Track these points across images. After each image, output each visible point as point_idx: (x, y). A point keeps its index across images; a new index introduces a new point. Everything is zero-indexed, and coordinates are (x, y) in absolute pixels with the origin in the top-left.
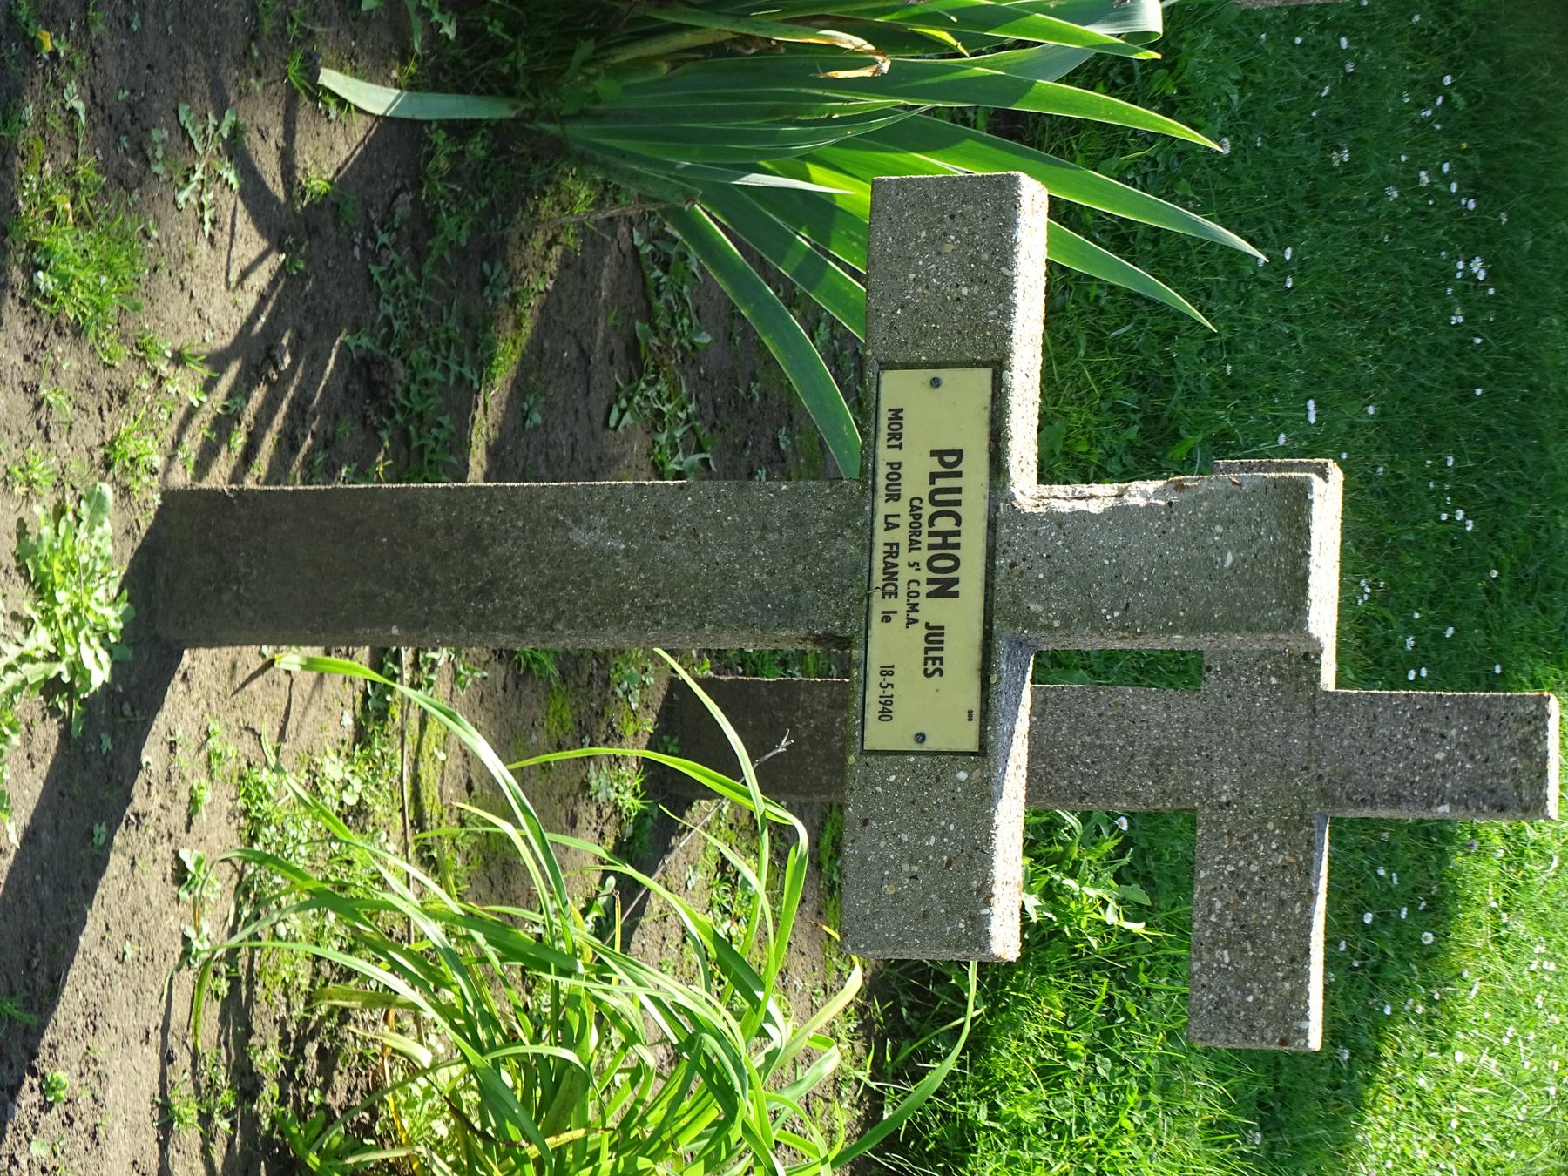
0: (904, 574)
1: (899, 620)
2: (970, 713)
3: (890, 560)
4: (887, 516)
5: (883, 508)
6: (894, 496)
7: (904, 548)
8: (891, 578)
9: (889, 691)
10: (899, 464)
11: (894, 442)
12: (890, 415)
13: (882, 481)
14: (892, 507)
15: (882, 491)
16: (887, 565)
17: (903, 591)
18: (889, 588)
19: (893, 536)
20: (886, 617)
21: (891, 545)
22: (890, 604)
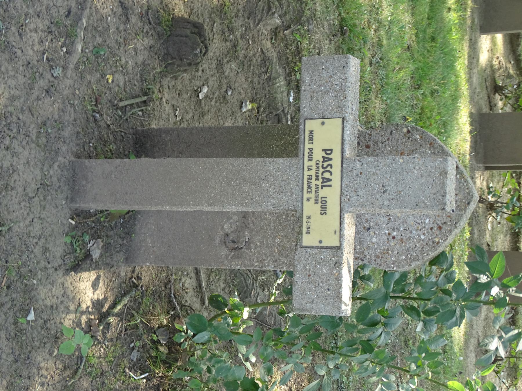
2: (335, 231)
3: (309, 181)
5: (307, 163)
6: (310, 159)
7: (314, 177)
8: (309, 187)
11: (310, 142)
13: (306, 155)
14: (310, 163)
15: (306, 158)
16: (309, 182)
17: (313, 192)
18: (309, 190)
19: (310, 173)
20: (308, 200)
22: (309, 195)
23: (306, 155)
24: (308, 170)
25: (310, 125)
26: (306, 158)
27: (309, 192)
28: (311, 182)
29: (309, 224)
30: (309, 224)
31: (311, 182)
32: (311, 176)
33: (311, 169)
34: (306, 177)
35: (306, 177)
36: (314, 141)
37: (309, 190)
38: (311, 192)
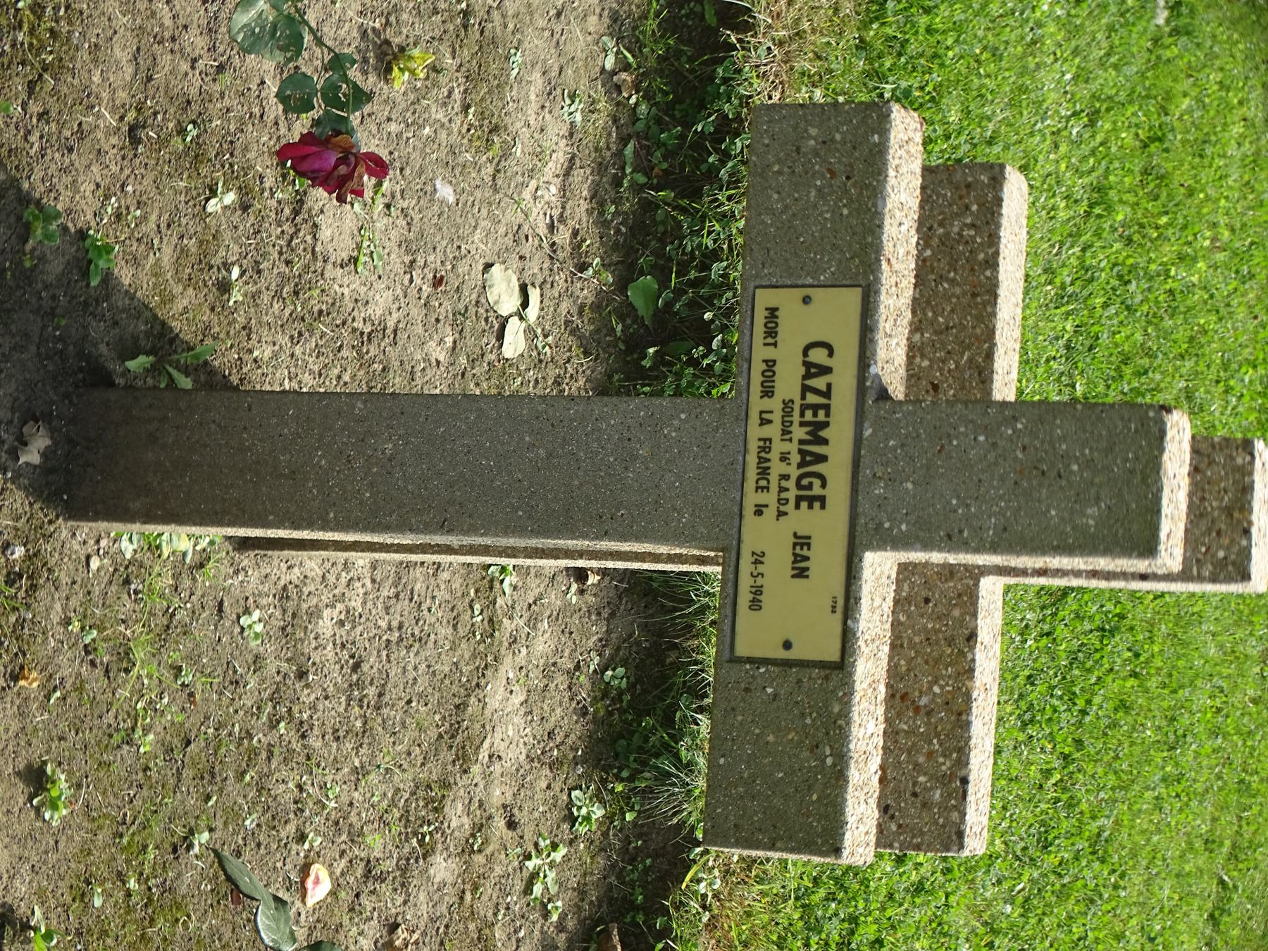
0: (777, 468)
1: (770, 513)
3: (763, 455)
4: (761, 412)
5: (757, 403)
6: (768, 393)
8: (764, 472)
9: (759, 583)
10: (774, 361)
11: (770, 340)
12: (766, 313)
14: (767, 403)
16: (762, 460)
18: (763, 483)
19: (767, 431)
20: (759, 512)
21: (765, 440)
22: (762, 498)
23: (756, 378)
24: (761, 424)
27: (762, 488)
28: (769, 460)
29: (760, 581)
30: (760, 581)
31: (769, 460)
32: (770, 440)
33: (770, 422)
34: (753, 446)
35: (753, 446)
37: (763, 483)
38: (768, 488)
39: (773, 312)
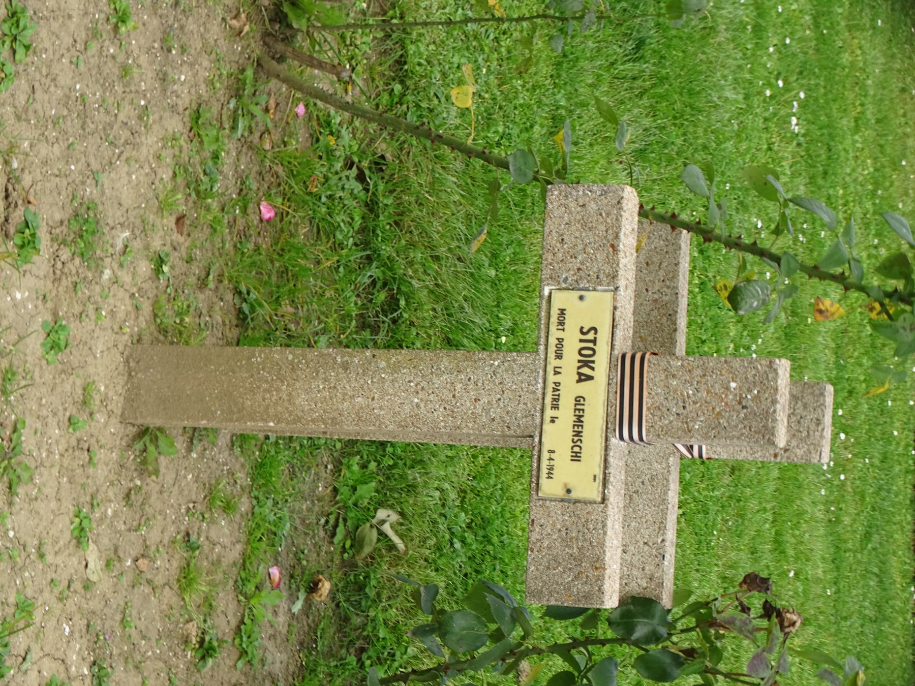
5: (553, 362)
6: (559, 356)
8: (556, 400)
11: (560, 327)
13: (552, 349)
14: (557, 363)
15: (552, 355)
19: (557, 378)
20: (553, 421)
23: (552, 349)
25: (561, 300)
26: (552, 355)
29: (552, 463)
33: (560, 373)
34: (550, 386)
35: (550, 386)
36: (565, 327)
39: (562, 312)
